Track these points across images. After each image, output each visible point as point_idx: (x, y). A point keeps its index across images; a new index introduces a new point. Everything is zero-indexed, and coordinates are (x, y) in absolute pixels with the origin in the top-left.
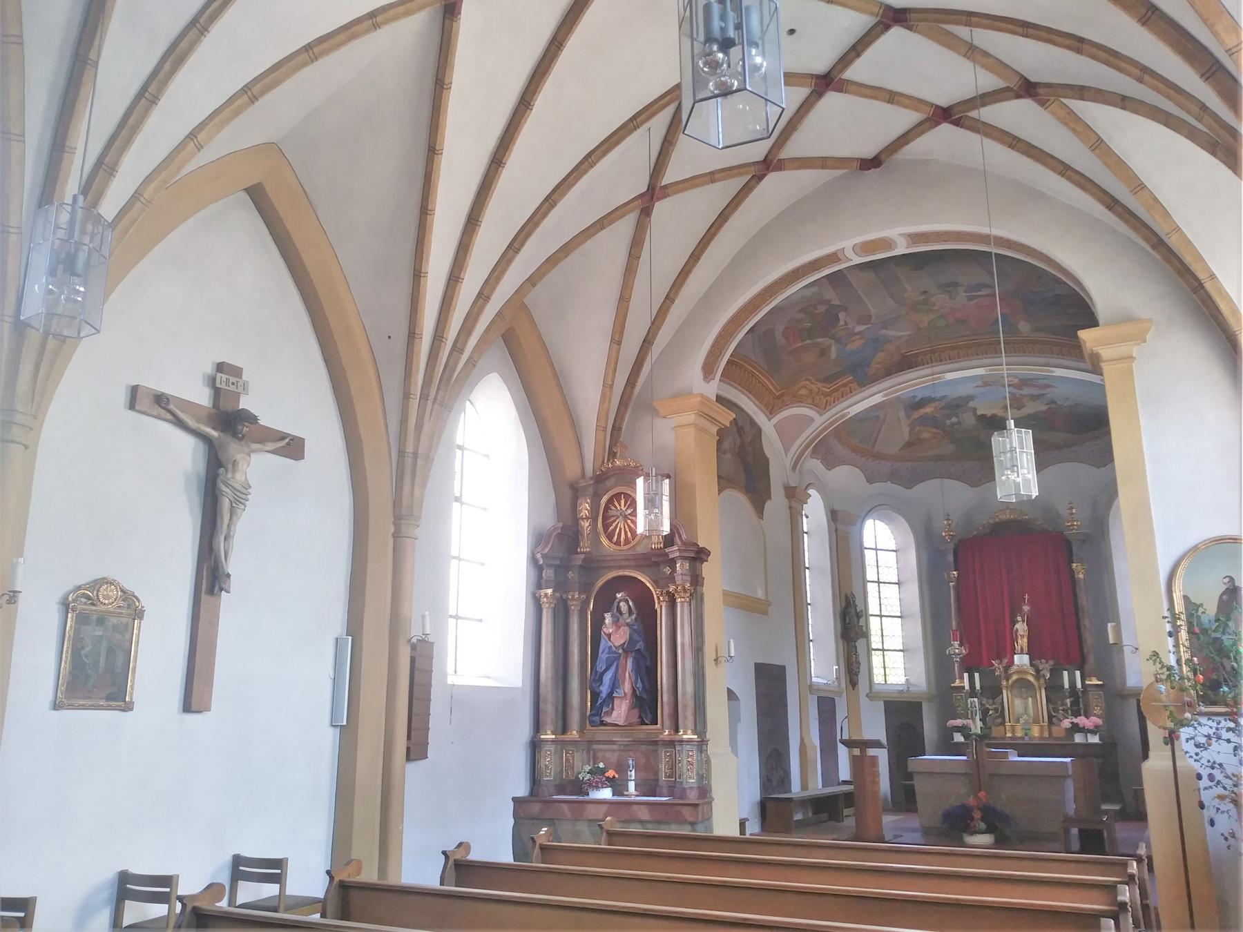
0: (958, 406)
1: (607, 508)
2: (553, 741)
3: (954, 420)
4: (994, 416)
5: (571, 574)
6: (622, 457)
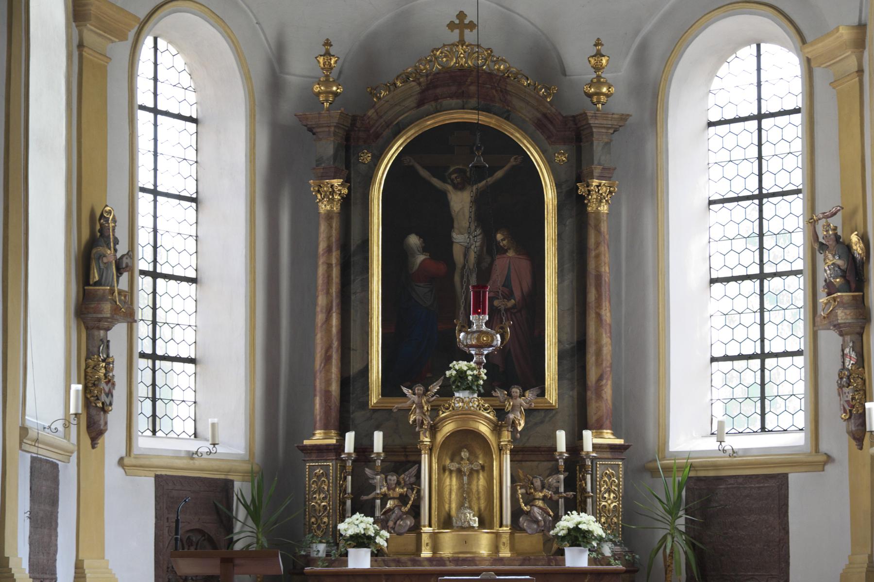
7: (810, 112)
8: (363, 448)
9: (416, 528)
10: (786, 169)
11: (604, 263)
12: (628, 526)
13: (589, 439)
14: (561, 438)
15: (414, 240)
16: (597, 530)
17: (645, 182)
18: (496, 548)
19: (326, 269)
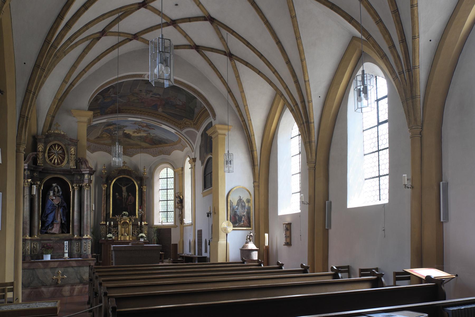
0: (120, 128)
1: (49, 150)
2: (30, 240)
3: (116, 132)
4: (129, 134)
5: (35, 174)
6: (57, 129)
7: (175, 178)
8: (110, 224)
9: (118, 236)
10: (171, 186)
11: (145, 198)
12: (148, 235)
13: (143, 223)
14: (139, 223)
15: (117, 194)
16: (145, 236)
17: (151, 187)
18: (129, 238)
19: (104, 197)
